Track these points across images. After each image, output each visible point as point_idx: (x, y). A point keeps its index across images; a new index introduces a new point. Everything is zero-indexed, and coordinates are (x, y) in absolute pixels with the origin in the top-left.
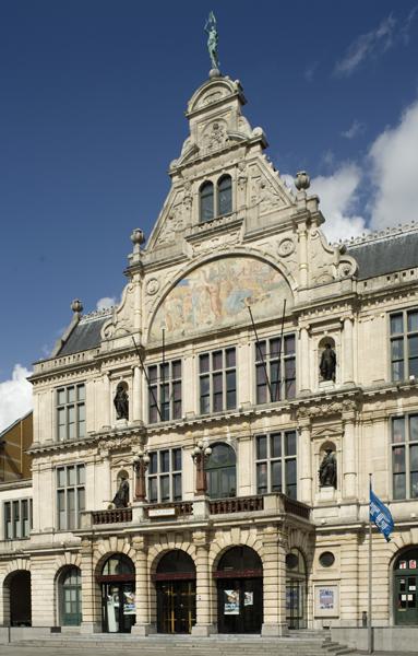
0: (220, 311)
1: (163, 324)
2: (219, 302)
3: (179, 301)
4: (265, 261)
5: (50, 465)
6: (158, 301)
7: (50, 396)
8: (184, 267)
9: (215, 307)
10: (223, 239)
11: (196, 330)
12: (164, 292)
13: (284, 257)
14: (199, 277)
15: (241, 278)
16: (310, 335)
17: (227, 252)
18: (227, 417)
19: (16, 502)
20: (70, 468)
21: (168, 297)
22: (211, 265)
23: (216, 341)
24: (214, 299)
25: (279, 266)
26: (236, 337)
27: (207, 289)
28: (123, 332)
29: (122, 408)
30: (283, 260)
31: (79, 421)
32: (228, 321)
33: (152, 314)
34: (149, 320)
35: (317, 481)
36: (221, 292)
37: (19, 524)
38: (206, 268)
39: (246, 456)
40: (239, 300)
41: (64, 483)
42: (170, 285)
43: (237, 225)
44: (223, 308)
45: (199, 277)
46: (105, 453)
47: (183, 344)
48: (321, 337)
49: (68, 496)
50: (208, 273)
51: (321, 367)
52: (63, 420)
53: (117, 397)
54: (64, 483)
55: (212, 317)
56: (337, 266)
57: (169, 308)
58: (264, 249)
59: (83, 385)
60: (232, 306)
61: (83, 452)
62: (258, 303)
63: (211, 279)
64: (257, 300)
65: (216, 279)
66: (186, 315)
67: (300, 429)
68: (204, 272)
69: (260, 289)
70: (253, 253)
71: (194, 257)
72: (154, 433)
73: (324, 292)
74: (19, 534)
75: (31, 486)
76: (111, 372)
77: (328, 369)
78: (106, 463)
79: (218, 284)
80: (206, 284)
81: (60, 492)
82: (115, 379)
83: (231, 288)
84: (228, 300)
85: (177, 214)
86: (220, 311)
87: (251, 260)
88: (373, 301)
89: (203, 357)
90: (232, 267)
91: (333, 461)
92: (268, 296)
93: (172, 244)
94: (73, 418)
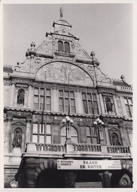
0: (66, 78)
3: (49, 70)
9: (64, 76)
12: (44, 64)
13: (90, 70)
14: (57, 65)
21: (44, 67)
27: (61, 70)
29: (21, 100)
38: (61, 64)
45: (57, 65)
50: (61, 65)
55: (63, 79)
63: (63, 67)
64: (80, 80)
66: (52, 75)
68: (59, 64)
76: (17, 83)
77: (109, 108)
80: (61, 69)
92: (84, 80)
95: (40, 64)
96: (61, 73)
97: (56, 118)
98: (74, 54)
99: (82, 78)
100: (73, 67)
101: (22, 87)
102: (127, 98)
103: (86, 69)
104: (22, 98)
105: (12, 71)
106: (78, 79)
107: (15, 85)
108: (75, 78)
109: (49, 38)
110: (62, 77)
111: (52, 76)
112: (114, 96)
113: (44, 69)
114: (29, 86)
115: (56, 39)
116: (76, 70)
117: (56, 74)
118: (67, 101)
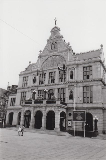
1: (43, 66)
5: (20, 91)
7: (22, 78)
8: (48, 57)
16: (69, 70)
18: (53, 84)
19: (13, 98)
20: (24, 92)
22: (52, 57)
24: (52, 63)
31: (27, 83)
35: (69, 98)
37: (13, 103)
39: (56, 92)
41: (22, 95)
46: (30, 90)
48: (71, 71)
49: (23, 98)
51: (70, 76)
52: (24, 83)
53: (34, 79)
54: (22, 95)
56: (74, 58)
58: (62, 54)
59: (28, 77)
61: (27, 89)
64: (60, 63)
67: (66, 88)
70: (60, 55)
74: (13, 105)
75: (16, 95)
76: (33, 75)
77: (72, 77)
81: (21, 97)
87: (59, 56)
88: (80, 64)
89: (50, 73)
91: (72, 94)
94: (26, 83)
112: (75, 68)
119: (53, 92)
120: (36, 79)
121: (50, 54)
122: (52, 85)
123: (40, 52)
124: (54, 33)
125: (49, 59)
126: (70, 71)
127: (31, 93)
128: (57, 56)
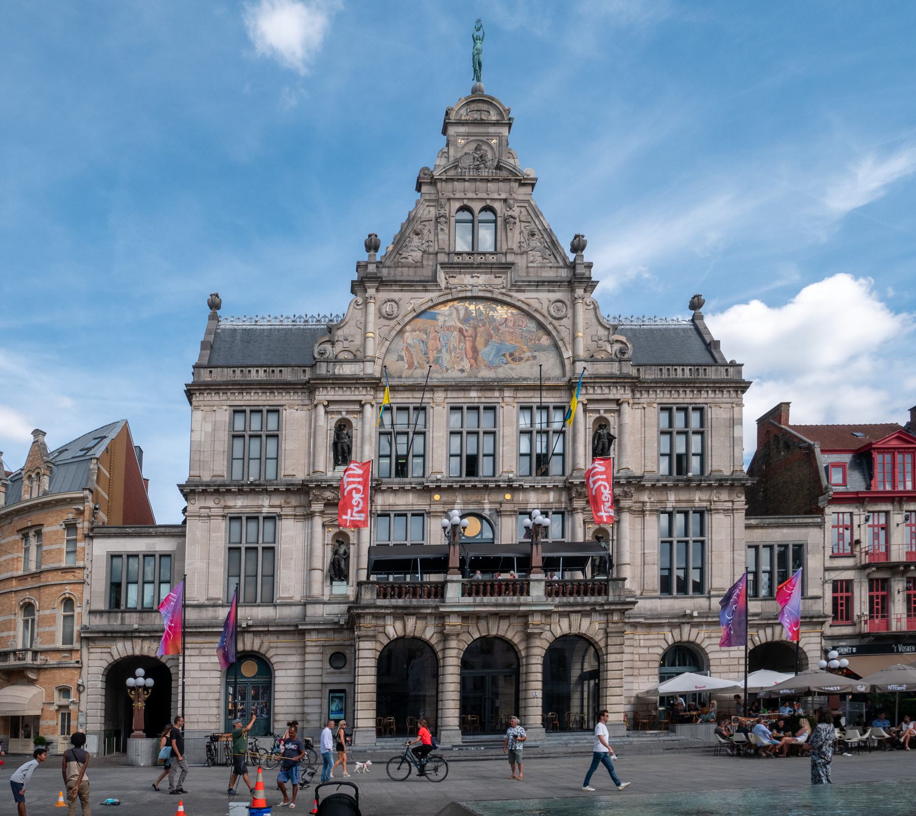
0: (476, 359)
2: (475, 350)
3: (425, 336)
4: (532, 317)
6: (398, 328)
9: (470, 354)
10: (482, 279)
11: (445, 375)
12: (407, 319)
14: (451, 315)
15: (503, 328)
17: (489, 295)
21: (408, 328)
22: (467, 304)
23: (473, 394)
24: (469, 344)
25: (550, 327)
26: (497, 394)
28: (350, 356)
30: (554, 322)
32: (485, 374)
33: (387, 343)
34: (384, 350)
36: (478, 339)
38: (460, 305)
40: (499, 353)
42: (415, 314)
43: (508, 267)
44: (480, 357)
45: (451, 315)
47: (432, 389)
50: (462, 313)
55: (466, 364)
57: (409, 341)
58: (536, 305)
60: (492, 355)
62: (522, 363)
63: (466, 319)
64: (521, 359)
65: (472, 321)
66: (432, 355)
68: (457, 309)
69: (525, 348)
70: (519, 304)
71: (447, 288)
72: (391, 490)
73: (603, 369)
78: (318, 521)
79: (475, 328)
80: (461, 326)
82: (332, 412)
83: (491, 338)
84: (486, 349)
85: (425, 232)
86: (476, 359)
87: (515, 311)
90: (491, 313)
92: (535, 357)
93: (418, 265)
95: (393, 323)
96: (460, 342)
97: (437, 497)
98: (510, 258)
99: (528, 354)
100: (501, 312)
101: (344, 413)
102: (670, 410)
103: (544, 316)
104: (346, 448)
105: (315, 358)
106: (513, 360)
107: (325, 406)
108: (504, 355)
109: (427, 204)
110: (462, 360)
111: (431, 359)
113: (407, 334)
114: (362, 406)
115: (449, 199)
116: (511, 324)
117: (444, 350)
118: (473, 439)
119: (481, 532)
120: (356, 435)
121: (452, 281)
122: (474, 487)
123: (372, 245)
124: (469, 135)
125: (441, 319)
126: (590, 423)
127: (324, 526)
128: (499, 308)
